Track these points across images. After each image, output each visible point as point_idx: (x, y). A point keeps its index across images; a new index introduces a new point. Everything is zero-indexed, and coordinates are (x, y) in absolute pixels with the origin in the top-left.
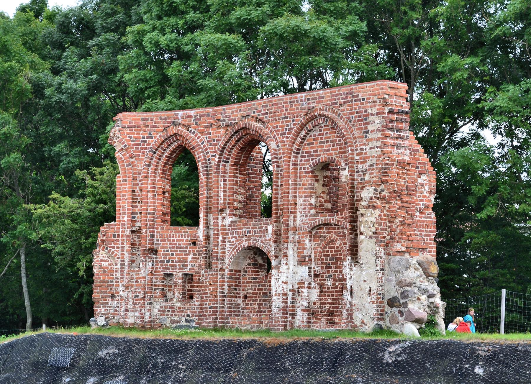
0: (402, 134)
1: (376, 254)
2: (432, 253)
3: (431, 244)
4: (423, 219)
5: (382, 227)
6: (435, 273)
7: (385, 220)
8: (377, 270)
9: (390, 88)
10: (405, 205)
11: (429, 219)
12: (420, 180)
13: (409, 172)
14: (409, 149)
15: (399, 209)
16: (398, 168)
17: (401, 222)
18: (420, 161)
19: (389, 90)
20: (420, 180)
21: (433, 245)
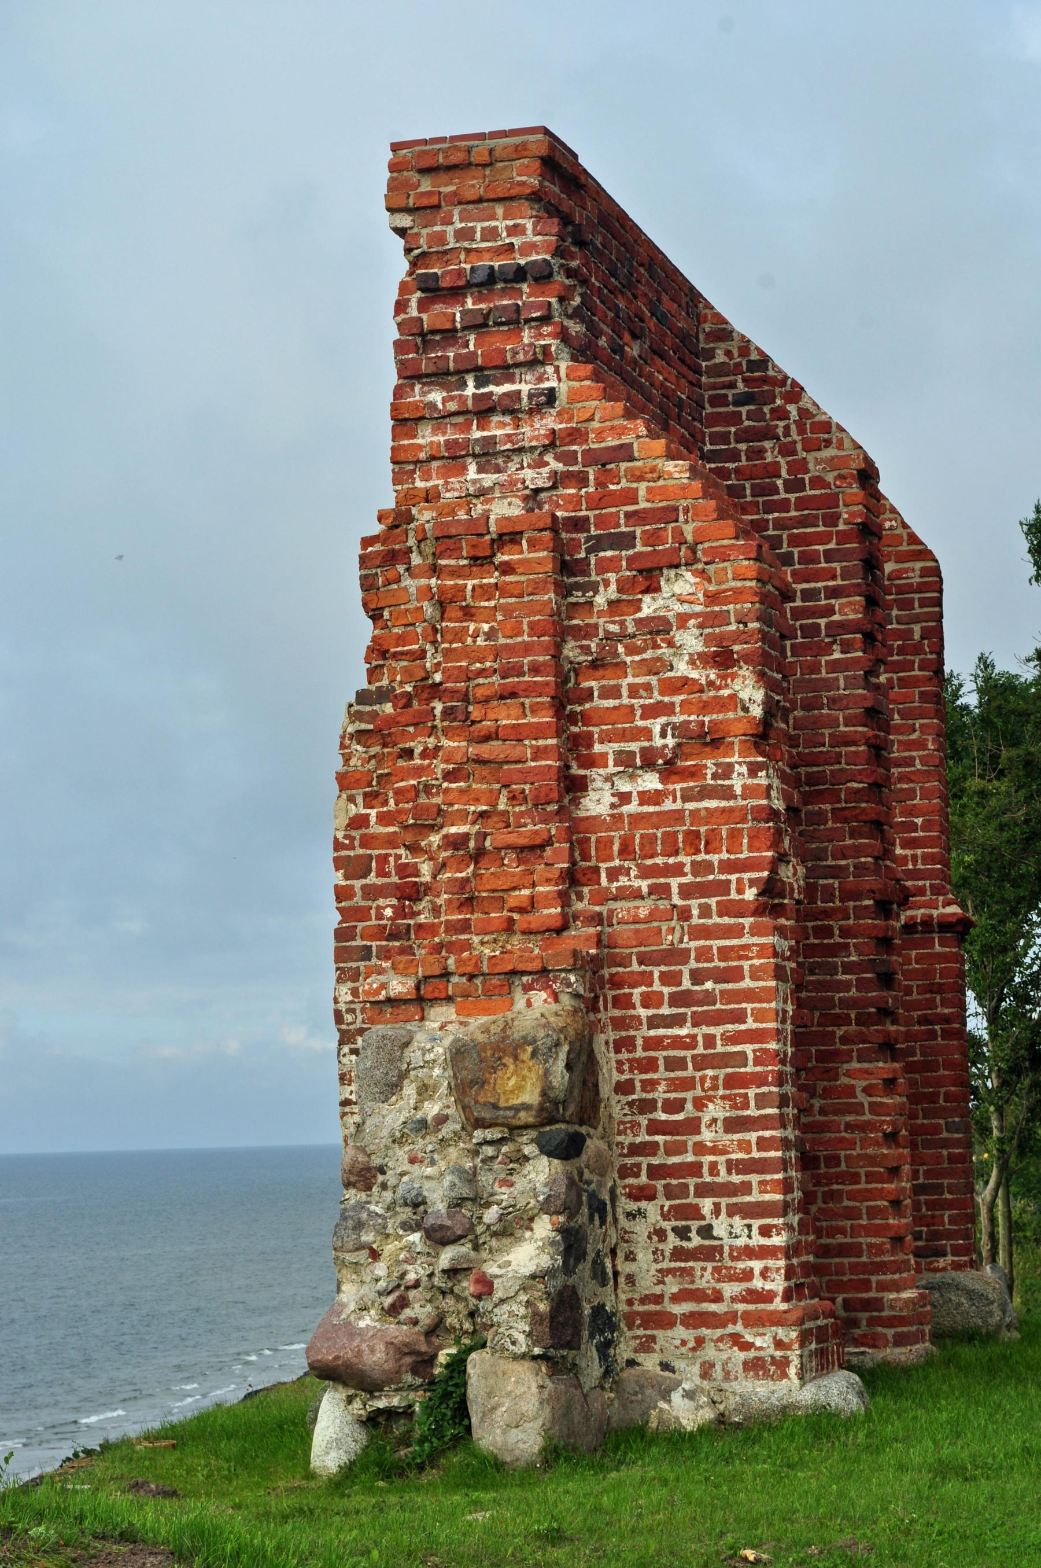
0: (499, 390)
1: (339, 1017)
2: (747, 983)
3: (736, 931)
4: (668, 805)
5: (372, 879)
6: (526, 1107)
7: (391, 841)
8: (346, 1103)
9: (423, 171)
10: (486, 750)
11: (713, 804)
12: (649, 607)
13: (508, 578)
14: (569, 458)
15: (448, 776)
16: (435, 570)
17: (457, 843)
18: (643, 505)
19: (426, 185)
20: (649, 607)
21: (747, 940)
